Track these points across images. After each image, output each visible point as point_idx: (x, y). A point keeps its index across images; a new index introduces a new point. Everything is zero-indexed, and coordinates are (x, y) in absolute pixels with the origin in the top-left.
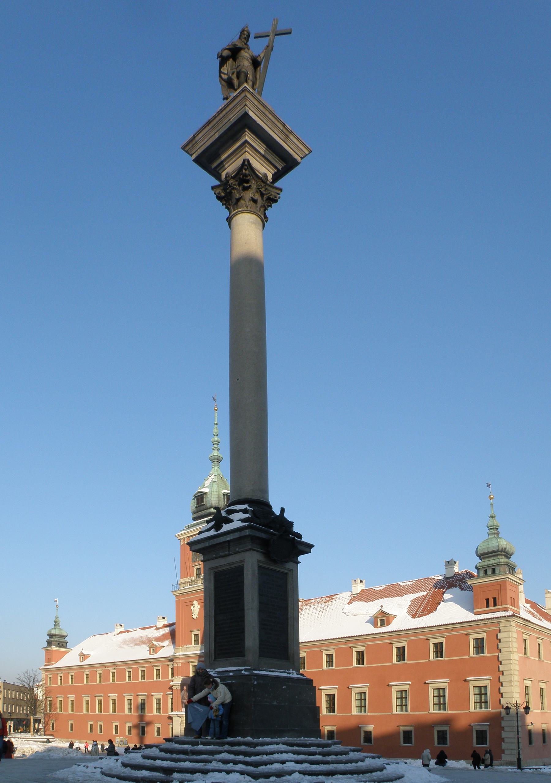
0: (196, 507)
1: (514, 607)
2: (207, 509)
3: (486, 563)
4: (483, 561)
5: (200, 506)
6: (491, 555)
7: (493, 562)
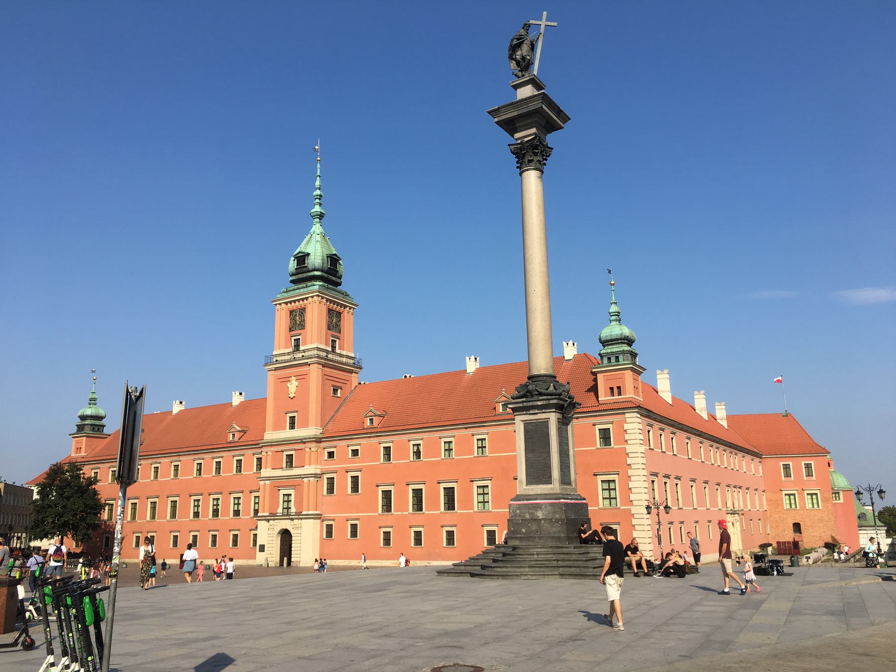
0: (296, 269)
2: (310, 271)
3: (609, 351)
4: (606, 348)
5: (301, 268)
6: (614, 342)
7: (617, 350)
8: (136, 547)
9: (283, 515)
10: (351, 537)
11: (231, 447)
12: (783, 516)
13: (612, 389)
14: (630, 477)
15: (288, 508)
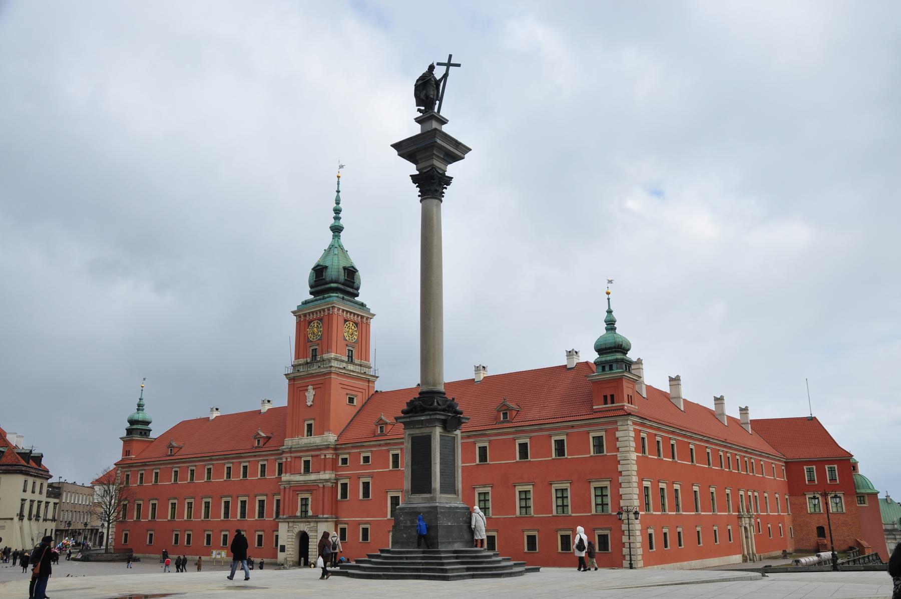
0: (315, 281)
1: (632, 404)
3: (603, 359)
6: (609, 351)
8: (175, 544)
9: (301, 517)
10: (363, 540)
11: (254, 452)
12: (807, 520)
13: (605, 397)
14: (621, 484)
15: (306, 512)
